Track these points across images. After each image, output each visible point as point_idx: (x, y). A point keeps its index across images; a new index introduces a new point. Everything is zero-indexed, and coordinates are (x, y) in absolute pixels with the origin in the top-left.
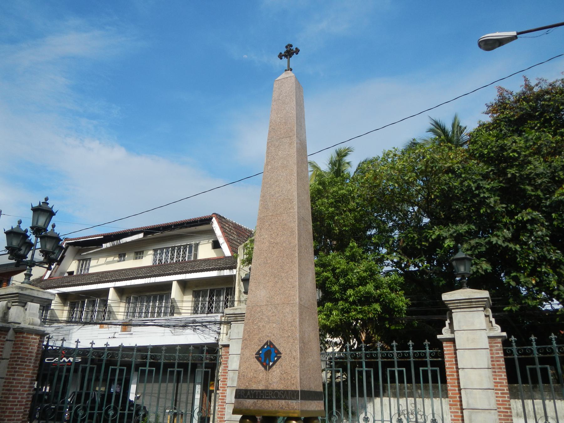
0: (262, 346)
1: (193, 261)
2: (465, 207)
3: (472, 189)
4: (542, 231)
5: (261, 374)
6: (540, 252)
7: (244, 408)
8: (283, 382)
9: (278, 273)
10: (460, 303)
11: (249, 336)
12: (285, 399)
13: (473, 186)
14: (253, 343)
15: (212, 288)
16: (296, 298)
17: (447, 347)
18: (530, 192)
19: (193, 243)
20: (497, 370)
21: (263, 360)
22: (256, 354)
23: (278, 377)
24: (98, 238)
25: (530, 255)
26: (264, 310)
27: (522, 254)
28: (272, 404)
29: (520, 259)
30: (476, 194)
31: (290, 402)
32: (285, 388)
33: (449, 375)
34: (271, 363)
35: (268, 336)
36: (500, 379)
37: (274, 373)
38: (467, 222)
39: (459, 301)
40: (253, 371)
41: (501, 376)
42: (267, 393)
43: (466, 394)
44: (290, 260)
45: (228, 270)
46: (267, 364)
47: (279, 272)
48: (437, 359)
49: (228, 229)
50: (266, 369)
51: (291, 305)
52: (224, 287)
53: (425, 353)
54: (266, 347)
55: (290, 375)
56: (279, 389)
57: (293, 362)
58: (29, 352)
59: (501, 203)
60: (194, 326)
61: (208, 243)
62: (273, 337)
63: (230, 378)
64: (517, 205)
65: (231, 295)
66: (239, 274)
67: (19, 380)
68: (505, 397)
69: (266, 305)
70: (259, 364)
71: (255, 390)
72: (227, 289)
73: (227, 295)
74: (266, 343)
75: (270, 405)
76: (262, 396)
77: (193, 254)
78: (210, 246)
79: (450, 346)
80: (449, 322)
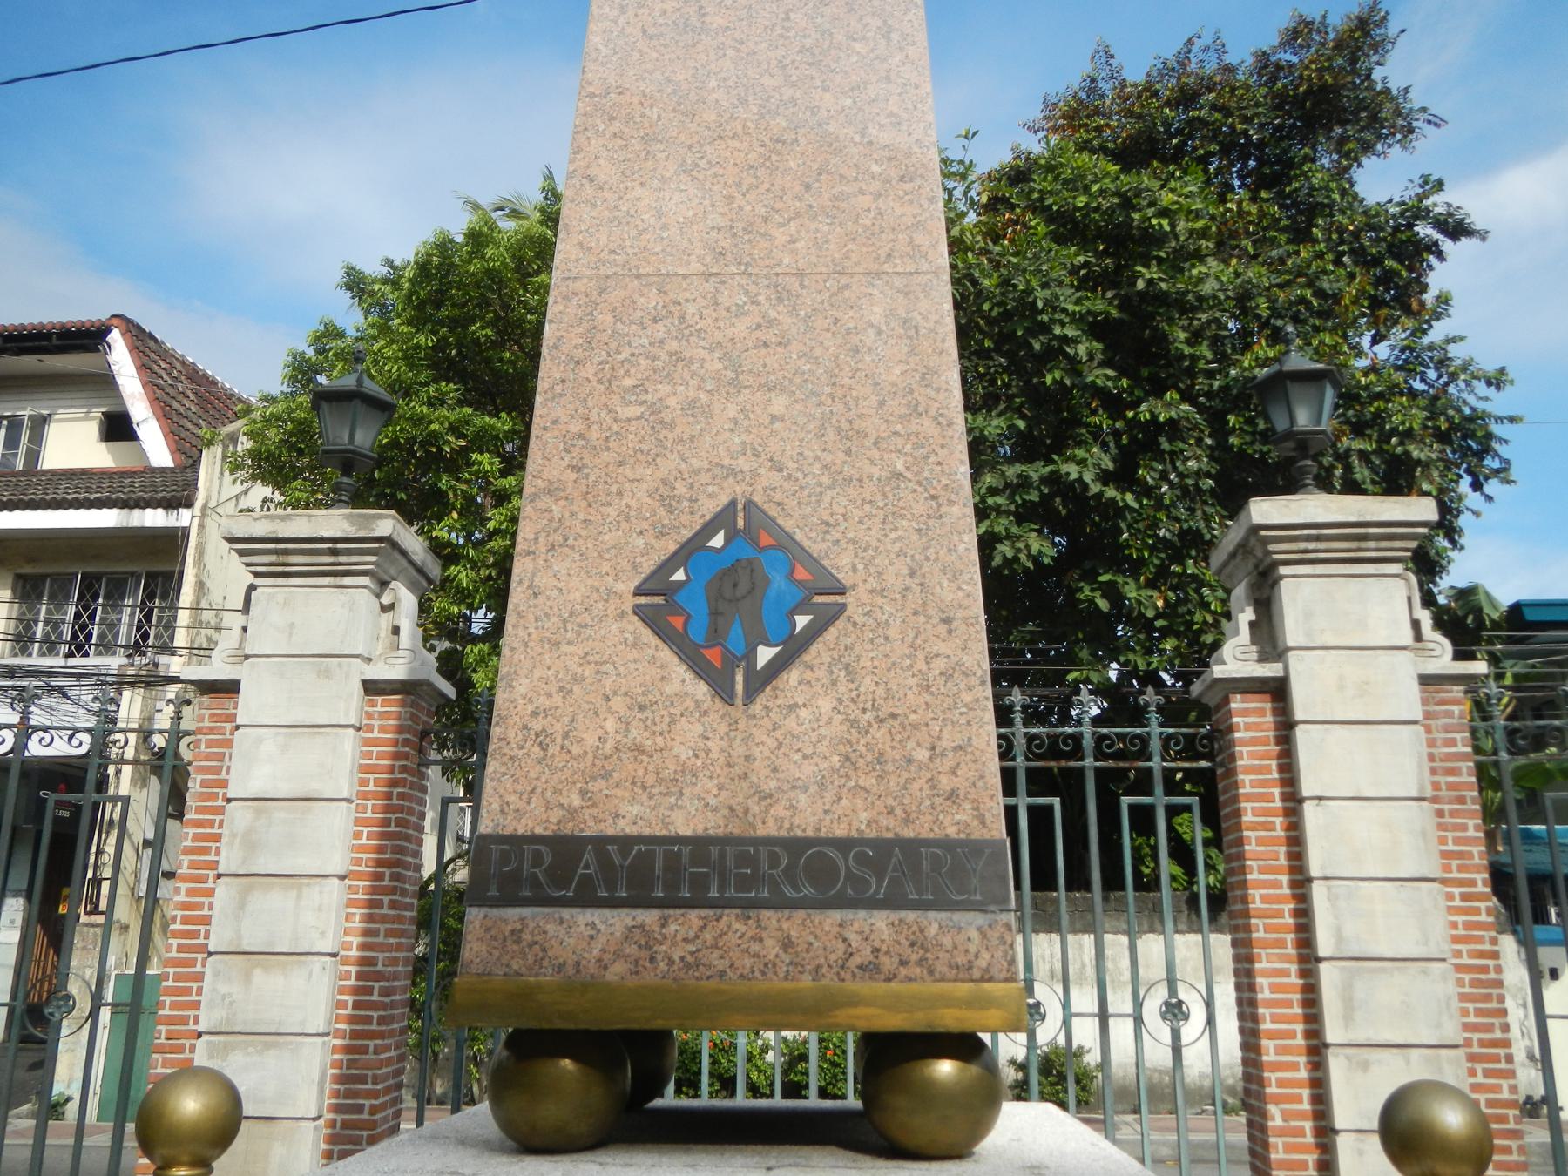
0: (687, 534)
1: (23, 473)
2: (981, 370)
3: (1034, 303)
4: (1198, 459)
5: (691, 730)
6: (1186, 521)
7: (548, 977)
8: (870, 782)
9: (788, 93)
10: (1318, 538)
11: (577, 469)
12: (892, 902)
13: (1041, 296)
14: (612, 512)
15: (90, 569)
16: (934, 246)
17: (1245, 713)
18: (1180, 346)
19: (27, 413)
20: (1446, 807)
21: (698, 633)
22: (638, 592)
23: (822, 749)
25: (1161, 525)
26: (691, 309)
27: (1137, 522)
28: (787, 944)
29: (1131, 535)
30: (1042, 322)
31: (933, 922)
32: (890, 827)
33: (1255, 827)
34: (765, 654)
35: (732, 472)
36: (1457, 841)
37: (791, 723)
38: (1002, 406)
39: (1317, 531)
40: (618, 703)
41: (1464, 828)
42: (743, 859)
43: (1333, 898)
44: (875, 22)
45: (160, 511)
46: (731, 662)
47: (792, 85)
48: (1194, 765)
49: (165, 376)
50: (723, 692)
51: (898, 282)
52: (142, 568)
53: (1144, 740)
54: (718, 541)
55: (922, 735)
56: (840, 831)
57: (942, 648)
59: (1102, 364)
60: (14, 688)
61: (87, 418)
62: (768, 478)
63: (234, 835)
64: (1136, 380)
65: (164, 597)
66: (201, 526)
68: (1477, 911)
69: (707, 276)
70: (666, 654)
71: (640, 839)
72: (152, 577)
73: (150, 596)
74: (724, 518)
75: (771, 948)
76: (700, 883)
77: (22, 451)
78: (92, 428)
79: (1261, 713)
80: (1253, 618)
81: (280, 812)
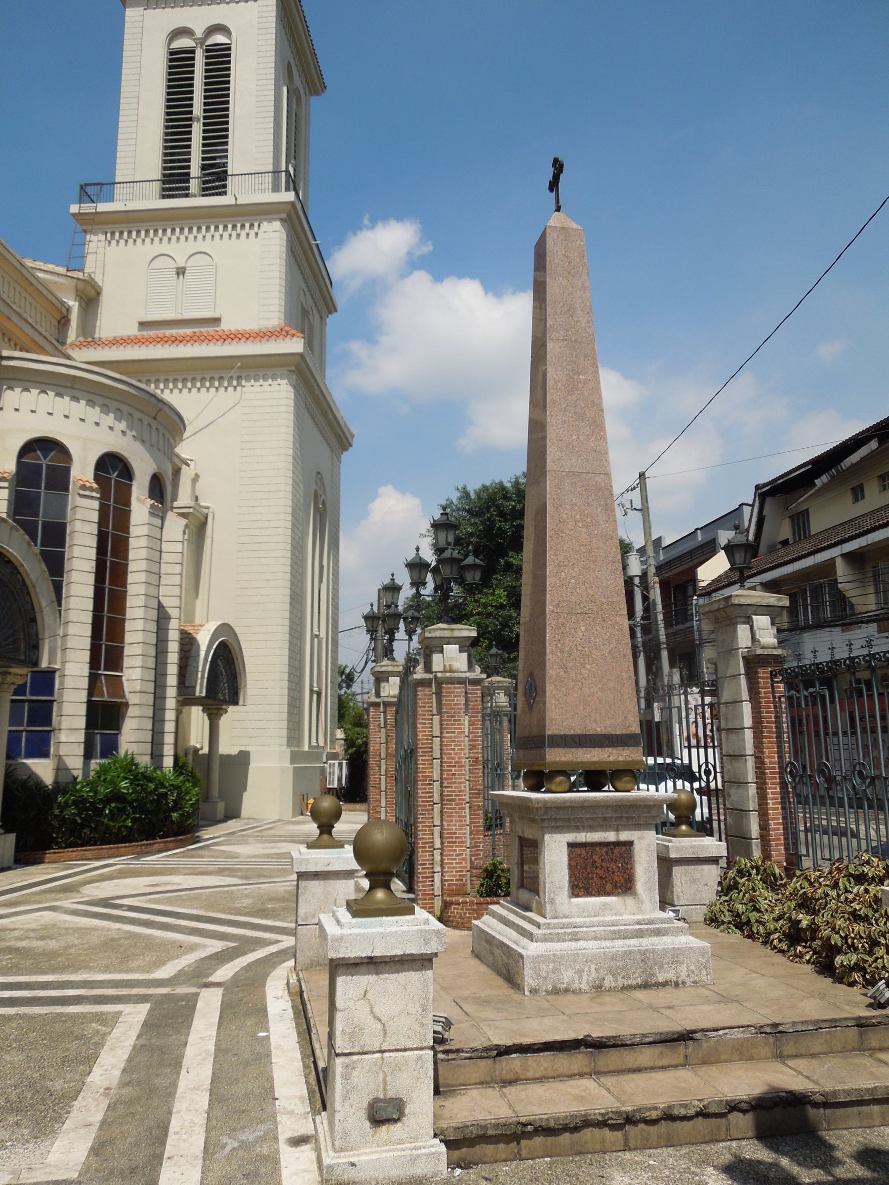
24: (807, 468)
58: (455, 705)
67: (451, 737)
81: (731, 707)
